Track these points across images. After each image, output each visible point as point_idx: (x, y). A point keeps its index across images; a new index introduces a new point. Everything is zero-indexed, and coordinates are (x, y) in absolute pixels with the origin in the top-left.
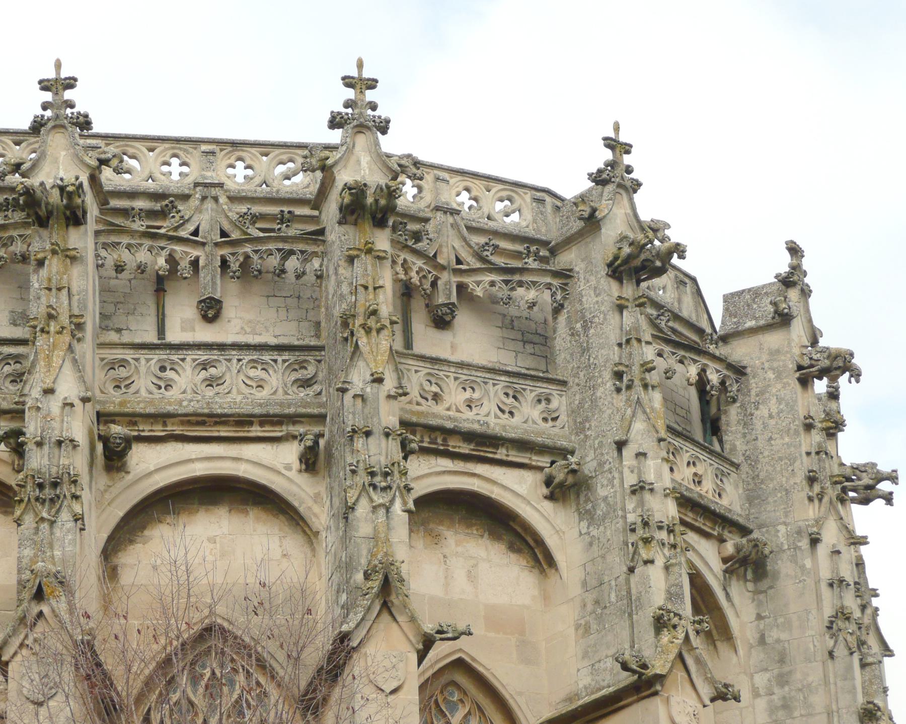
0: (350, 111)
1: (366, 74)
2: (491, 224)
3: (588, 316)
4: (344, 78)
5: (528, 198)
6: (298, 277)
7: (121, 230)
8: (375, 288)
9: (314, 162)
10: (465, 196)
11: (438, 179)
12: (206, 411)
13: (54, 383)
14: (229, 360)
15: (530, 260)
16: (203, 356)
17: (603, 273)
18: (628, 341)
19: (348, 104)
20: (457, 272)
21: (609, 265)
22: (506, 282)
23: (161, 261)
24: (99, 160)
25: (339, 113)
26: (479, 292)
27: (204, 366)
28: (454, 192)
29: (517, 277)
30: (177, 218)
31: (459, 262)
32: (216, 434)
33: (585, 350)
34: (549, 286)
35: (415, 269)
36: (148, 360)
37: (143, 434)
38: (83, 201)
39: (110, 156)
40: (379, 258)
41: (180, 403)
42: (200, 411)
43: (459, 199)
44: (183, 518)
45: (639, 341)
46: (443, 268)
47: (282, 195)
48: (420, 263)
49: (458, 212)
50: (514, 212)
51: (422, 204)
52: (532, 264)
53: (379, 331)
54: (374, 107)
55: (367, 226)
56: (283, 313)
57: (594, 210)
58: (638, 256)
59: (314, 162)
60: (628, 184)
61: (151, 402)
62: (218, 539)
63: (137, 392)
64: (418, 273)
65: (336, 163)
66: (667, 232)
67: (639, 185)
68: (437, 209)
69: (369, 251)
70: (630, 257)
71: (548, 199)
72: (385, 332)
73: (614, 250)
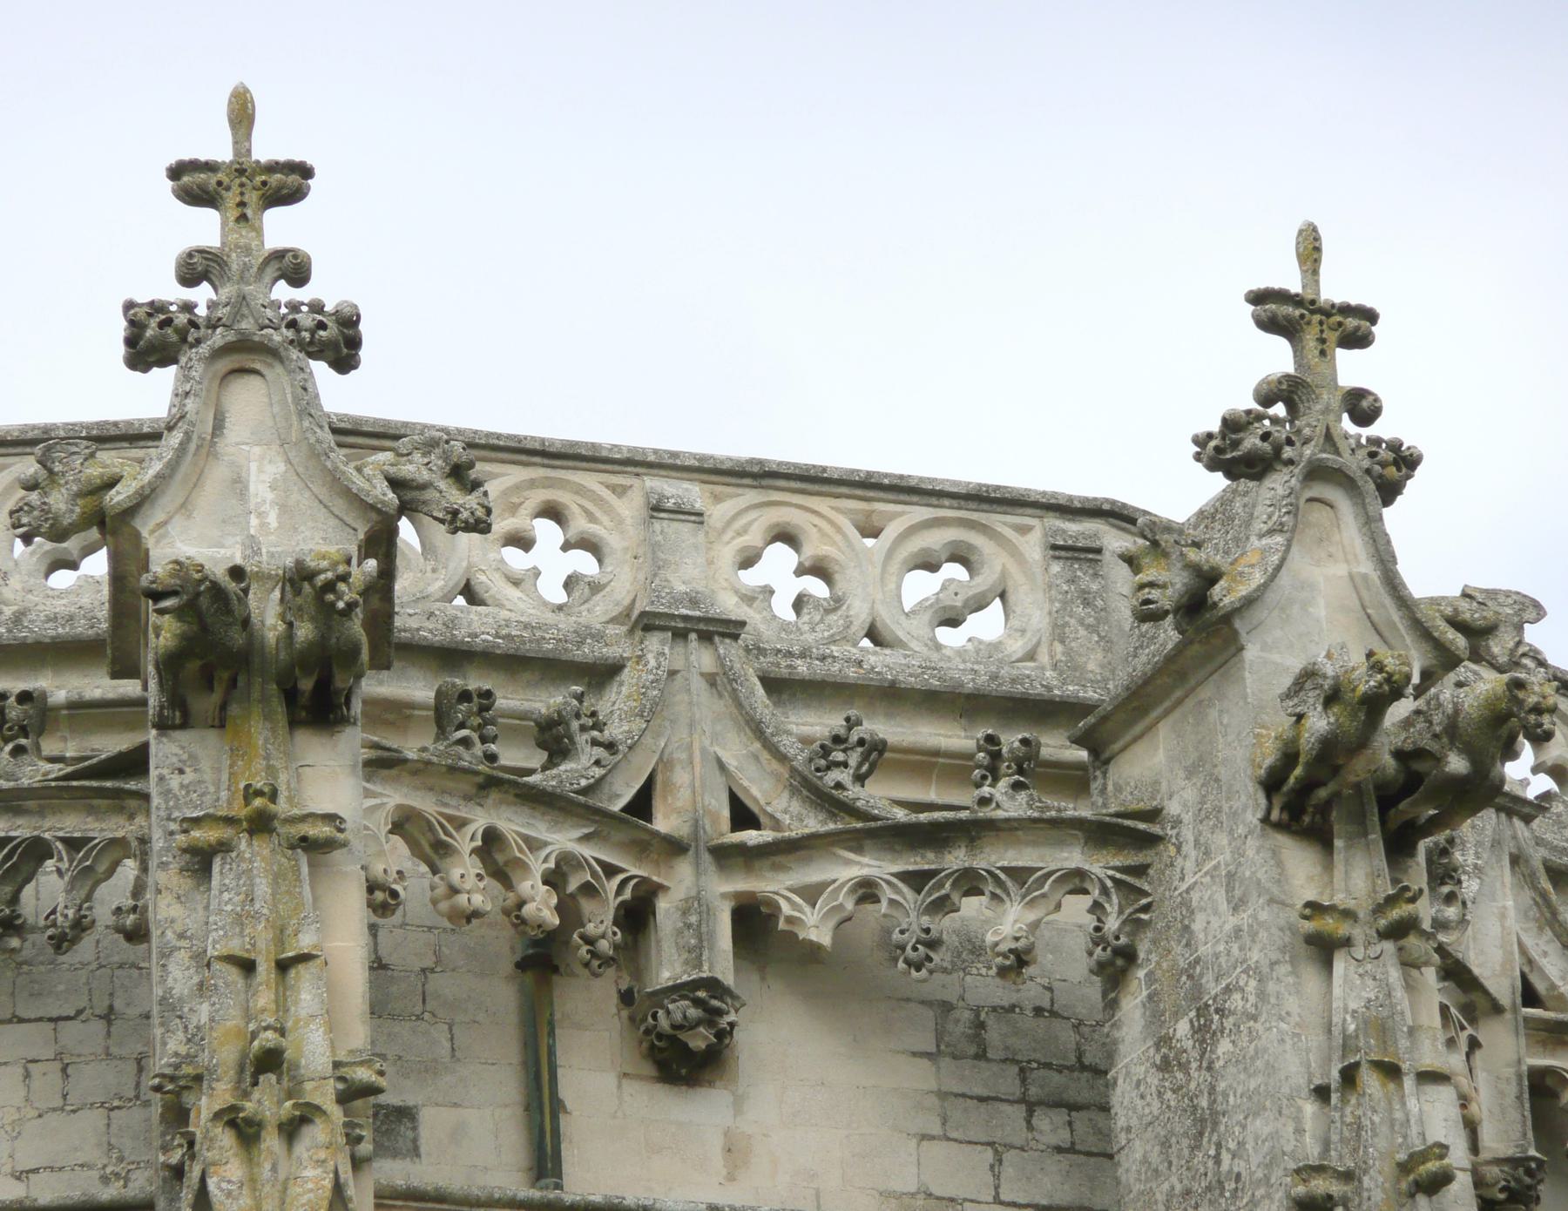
0: (202, 295)
1: (265, 148)
2: (881, 662)
3: (1213, 988)
4: (176, 172)
5: (1032, 546)
6: (62, 942)
8: (283, 966)
9: (59, 500)
10: (778, 564)
11: (656, 508)
15: (1000, 790)
17: (1253, 817)
18: (1349, 1076)
19: (194, 269)
20: (725, 856)
21: (1271, 784)
22: (916, 880)
25: (156, 308)
26: (816, 928)
28: (727, 553)
29: (956, 859)
31: (743, 816)
33: (1205, 1123)
34: (1076, 881)
35: (538, 865)
40: (307, 844)
43: (751, 578)
45: (1391, 1071)
46: (674, 847)
47: (37, 628)
48: (564, 839)
49: (731, 629)
50: (979, 604)
51: (598, 612)
52: (1010, 804)
53: (291, 1130)
54: (296, 270)
55: (261, 731)
56: (47, 1081)
57: (1210, 577)
58: (1362, 742)
59: (59, 500)
60: (1355, 463)
64: (554, 879)
65: (143, 499)
66: (1534, 635)
67: (1407, 461)
68: (647, 623)
69: (261, 824)
70: (1331, 753)
71: (1115, 541)
72: (316, 1134)
73: (1282, 723)
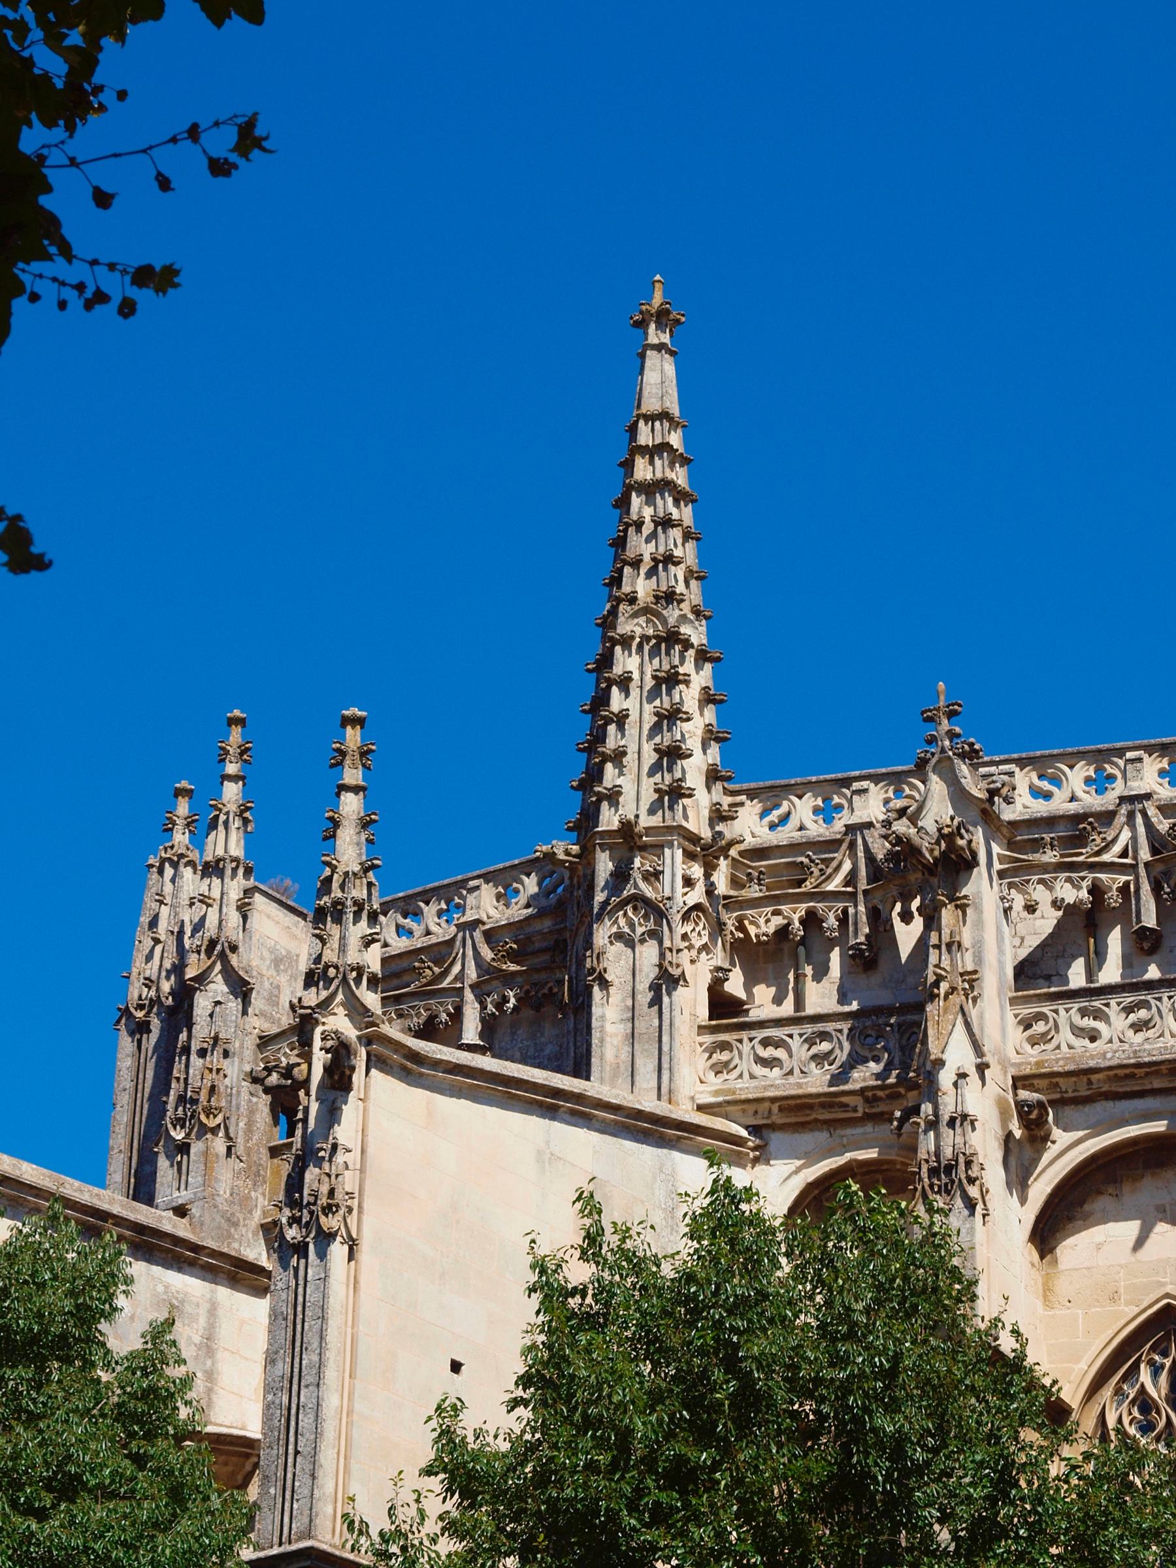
7: (1032, 868)
12: (1132, 1061)
13: (943, 1052)
14: (1159, 999)
16: (1129, 999)
23: (1084, 894)
24: (988, 791)
27: (1129, 1010)
30: (1098, 841)
32: (1148, 1087)
36: (1067, 1010)
37: (1065, 1095)
38: (970, 842)
39: (999, 785)
41: (1104, 1055)
42: (1125, 1062)
44: (1126, 1188)
61: (1072, 1059)
62: (1168, 1208)
63: (1058, 1047)
